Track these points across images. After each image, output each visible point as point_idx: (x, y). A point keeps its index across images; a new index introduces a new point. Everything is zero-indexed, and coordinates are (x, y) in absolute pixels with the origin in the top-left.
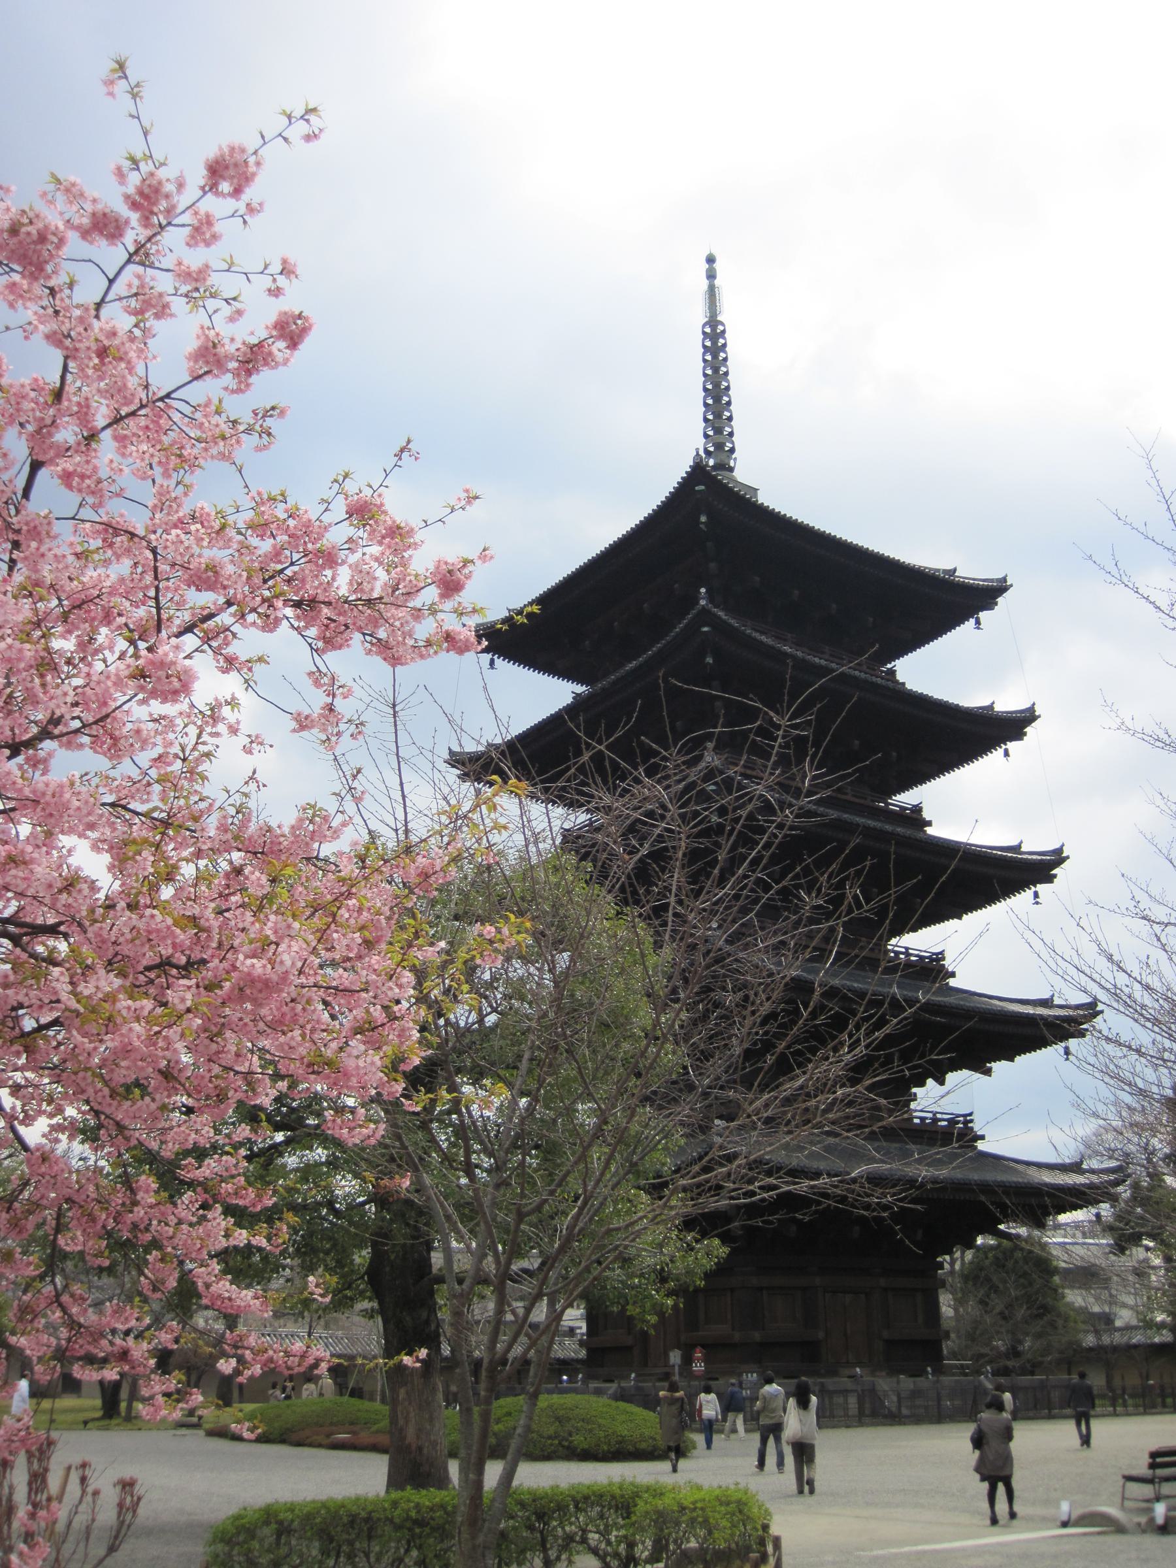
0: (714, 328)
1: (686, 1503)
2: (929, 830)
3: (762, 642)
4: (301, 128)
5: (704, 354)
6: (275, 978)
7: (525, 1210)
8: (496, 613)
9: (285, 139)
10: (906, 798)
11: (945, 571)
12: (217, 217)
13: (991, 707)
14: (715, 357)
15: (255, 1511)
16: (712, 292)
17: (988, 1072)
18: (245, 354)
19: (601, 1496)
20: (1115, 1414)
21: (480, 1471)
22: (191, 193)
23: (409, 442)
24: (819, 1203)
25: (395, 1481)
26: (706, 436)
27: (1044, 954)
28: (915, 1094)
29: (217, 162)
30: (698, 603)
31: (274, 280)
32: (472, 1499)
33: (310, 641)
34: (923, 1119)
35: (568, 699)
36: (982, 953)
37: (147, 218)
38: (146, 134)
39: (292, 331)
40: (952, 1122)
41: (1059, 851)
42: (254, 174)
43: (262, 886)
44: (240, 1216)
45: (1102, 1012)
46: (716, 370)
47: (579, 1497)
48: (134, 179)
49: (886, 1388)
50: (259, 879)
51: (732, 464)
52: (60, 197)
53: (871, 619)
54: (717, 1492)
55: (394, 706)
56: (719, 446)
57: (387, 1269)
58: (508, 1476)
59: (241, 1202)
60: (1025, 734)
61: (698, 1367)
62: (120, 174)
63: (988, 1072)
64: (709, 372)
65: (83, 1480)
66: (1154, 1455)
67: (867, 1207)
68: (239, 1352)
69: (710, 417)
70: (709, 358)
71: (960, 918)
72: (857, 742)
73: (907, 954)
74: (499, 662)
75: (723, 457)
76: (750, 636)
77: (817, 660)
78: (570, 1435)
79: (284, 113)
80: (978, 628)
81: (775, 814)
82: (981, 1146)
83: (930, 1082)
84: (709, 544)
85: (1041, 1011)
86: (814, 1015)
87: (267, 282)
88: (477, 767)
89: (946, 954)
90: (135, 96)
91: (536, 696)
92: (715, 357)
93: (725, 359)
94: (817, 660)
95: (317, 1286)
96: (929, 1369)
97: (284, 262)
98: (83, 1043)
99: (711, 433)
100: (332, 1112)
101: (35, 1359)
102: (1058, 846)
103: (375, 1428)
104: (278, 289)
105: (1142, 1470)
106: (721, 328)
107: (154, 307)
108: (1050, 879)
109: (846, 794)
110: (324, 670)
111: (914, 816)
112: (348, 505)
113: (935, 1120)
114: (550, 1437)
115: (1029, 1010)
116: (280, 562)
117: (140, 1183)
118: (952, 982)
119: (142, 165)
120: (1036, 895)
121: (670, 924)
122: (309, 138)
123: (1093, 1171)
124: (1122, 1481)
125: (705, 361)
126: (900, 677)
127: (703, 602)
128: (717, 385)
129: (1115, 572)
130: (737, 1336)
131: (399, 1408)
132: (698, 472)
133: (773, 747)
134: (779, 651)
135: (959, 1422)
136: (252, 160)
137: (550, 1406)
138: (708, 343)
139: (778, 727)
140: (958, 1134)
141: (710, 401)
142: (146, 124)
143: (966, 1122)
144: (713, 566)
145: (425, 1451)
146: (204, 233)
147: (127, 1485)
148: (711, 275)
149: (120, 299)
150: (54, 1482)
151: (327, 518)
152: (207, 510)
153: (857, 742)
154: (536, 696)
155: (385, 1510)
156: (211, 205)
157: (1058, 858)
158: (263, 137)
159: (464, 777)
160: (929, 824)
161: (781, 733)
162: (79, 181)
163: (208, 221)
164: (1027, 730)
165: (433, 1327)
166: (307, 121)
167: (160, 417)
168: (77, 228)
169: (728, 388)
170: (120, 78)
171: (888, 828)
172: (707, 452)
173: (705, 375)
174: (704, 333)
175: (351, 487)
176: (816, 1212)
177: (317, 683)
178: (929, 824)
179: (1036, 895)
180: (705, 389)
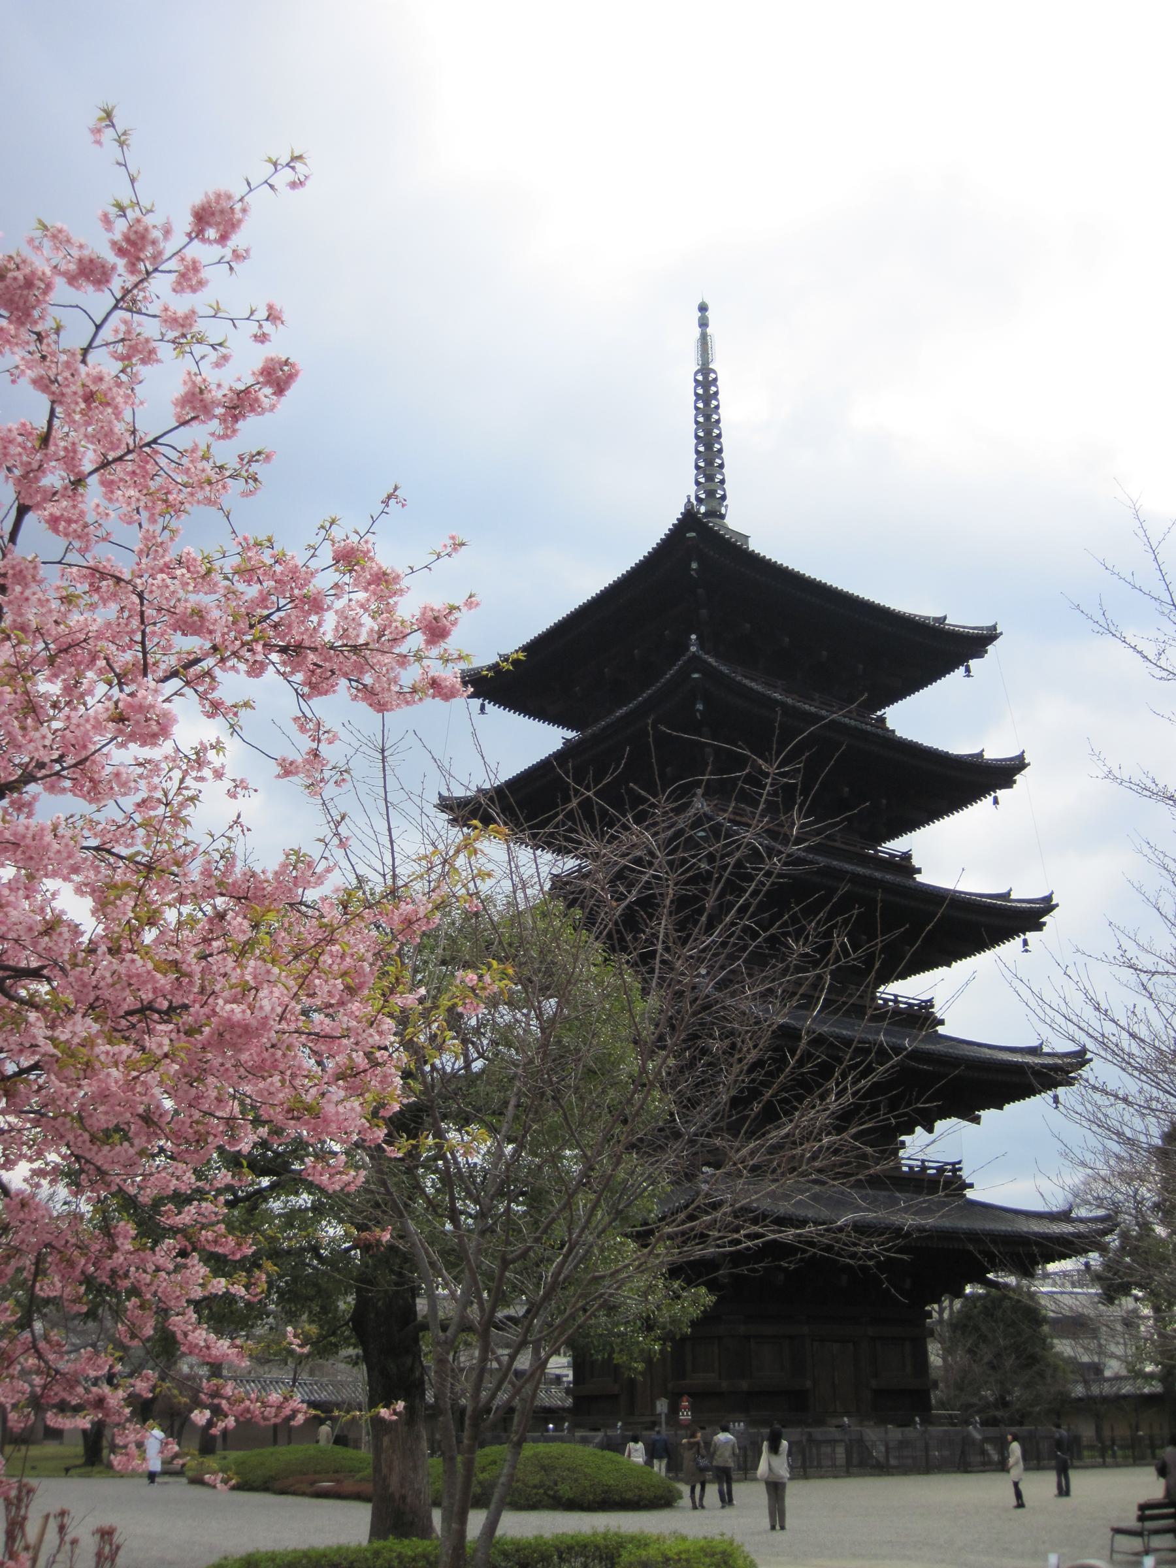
0: (706, 376)
1: (670, 1554)
3: (752, 689)
4: (286, 175)
5: (696, 402)
6: (254, 1023)
7: (510, 1257)
8: (484, 658)
9: (271, 186)
11: (936, 619)
12: (204, 263)
13: (981, 754)
14: (707, 404)
15: (236, 1561)
16: (704, 340)
17: (976, 1120)
18: (232, 400)
19: (585, 1546)
20: (1104, 1465)
21: (463, 1521)
22: (178, 239)
23: (396, 489)
24: (804, 1251)
25: (377, 1531)
26: (698, 483)
27: (1033, 1003)
28: (903, 1143)
29: (203, 209)
30: (688, 649)
31: (261, 326)
32: (455, 1549)
33: (296, 686)
34: (911, 1167)
35: (558, 745)
36: (971, 1000)
37: (134, 265)
38: (133, 181)
39: (278, 377)
40: (940, 1170)
41: (1049, 898)
42: (240, 221)
43: (244, 932)
44: (219, 1264)
45: (1091, 1060)
46: (708, 418)
47: (563, 1547)
48: (121, 226)
49: (874, 1438)
50: (241, 924)
51: (723, 511)
52: (47, 244)
53: (861, 666)
54: (702, 1543)
55: (383, 751)
56: (711, 494)
57: (372, 1316)
58: (492, 1525)
59: (220, 1250)
60: (1015, 782)
61: (685, 1416)
62: (106, 220)
63: (976, 1120)
64: (701, 419)
65: (62, 1528)
66: (1143, 1507)
67: (853, 1256)
68: (216, 1401)
69: (702, 464)
70: (700, 405)
71: (949, 965)
72: (847, 789)
73: (896, 1001)
74: (490, 707)
75: (714, 504)
76: (739, 683)
77: (807, 707)
78: (556, 1484)
79: (270, 160)
80: (968, 676)
81: (763, 862)
82: (970, 1194)
83: (919, 1130)
84: (700, 591)
85: (1029, 1059)
86: (801, 1063)
87: (253, 328)
88: (467, 811)
89: (935, 1002)
90: (122, 144)
91: (525, 742)
92: (707, 404)
93: (717, 407)
94: (807, 707)
95: (296, 1336)
96: (917, 1419)
97: (270, 308)
98: (61, 1088)
99: (702, 480)
100: (312, 1159)
101: (9, 1407)
102: (1047, 894)
103: (358, 1476)
104: (264, 335)
105: (1131, 1522)
106: (713, 376)
107: (140, 352)
108: (1039, 927)
109: (835, 841)
110: (310, 715)
111: (904, 863)
112: (335, 552)
113: (924, 1168)
114: (535, 1487)
115: (1018, 1058)
116: (267, 608)
117: (119, 1229)
118: (941, 1030)
119: (129, 212)
120: (1025, 943)
121: (657, 971)
122: (294, 185)
123: (1081, 1220)
124: (1110, 1534)
125: (697, 408)
126: (890, 725)
127: (693, 649)
128: (708, 433)
129: (1102, 621)
130: (725, 1385)
131: (383, 1456)
132: (689, 519)
133: (761, 795)
134: (769, 698)
135: (948, 1472)
136: (238, 206)
137: (536, 1455)
138: (700, 391)
139: (767, 775)
140: (947, 1182)
141: (702, 449)
142: (133, 171)
143: (954, 1171)
144: (703, 612)
145: (409, 1500)
146: (190, 279)
147: (106, 1534)
148: (703, 324)
149: (107, 344)
150: (32, 1530)
151: (314, 564)
152: (193, 555)
153: (847, 789)
154: (525, 742)
155: (367, 1559)
156: (198, 251)
157: (1046, 906)
158: (249, 184)
159: (454, 822)
160: (919, 871)
161: (769, 781)
162: (65, 227)
163: (195, 267)
164: (1017, 777)
165: (417, 1374)
166: (293, 168)
167: (147, 462)
168: (64, 274)
169: (719, 436)
170: (107, 126)
171: (878, 875)
172: (698, 499)
173: (697, 422)
174: (696, 381)
175: (337, 533)
176: (802, 1260)
177: (303, 729)
178: (919, 871)
179: (1025, 943)
180: (697, 437)
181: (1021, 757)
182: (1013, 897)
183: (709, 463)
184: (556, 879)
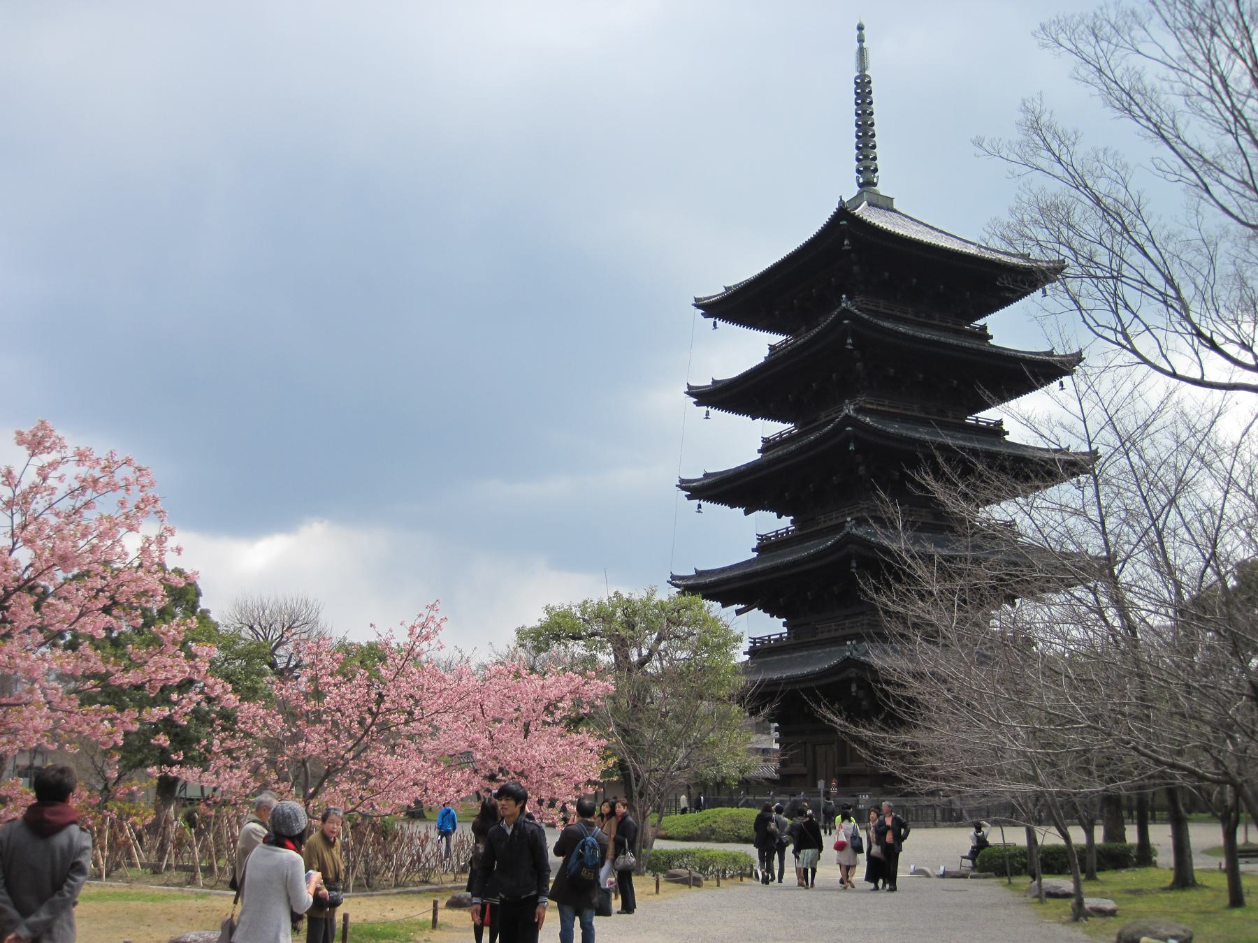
10: (989, 415)
14: (863, 101)
16: (862, 52)
46: (864, 112)
74: (720, 323)
92: (863, 101)
126: (989, 332)
128: (865, 123)
132: (843, 213)
134: (897, 332)
144: (856, 268)
148: (861, 40)
159: (698, 404)
160: (1007, 433)
172: (858, 171)
178: (1007, 433)
181: (1080, 352)
184: (765, 440)
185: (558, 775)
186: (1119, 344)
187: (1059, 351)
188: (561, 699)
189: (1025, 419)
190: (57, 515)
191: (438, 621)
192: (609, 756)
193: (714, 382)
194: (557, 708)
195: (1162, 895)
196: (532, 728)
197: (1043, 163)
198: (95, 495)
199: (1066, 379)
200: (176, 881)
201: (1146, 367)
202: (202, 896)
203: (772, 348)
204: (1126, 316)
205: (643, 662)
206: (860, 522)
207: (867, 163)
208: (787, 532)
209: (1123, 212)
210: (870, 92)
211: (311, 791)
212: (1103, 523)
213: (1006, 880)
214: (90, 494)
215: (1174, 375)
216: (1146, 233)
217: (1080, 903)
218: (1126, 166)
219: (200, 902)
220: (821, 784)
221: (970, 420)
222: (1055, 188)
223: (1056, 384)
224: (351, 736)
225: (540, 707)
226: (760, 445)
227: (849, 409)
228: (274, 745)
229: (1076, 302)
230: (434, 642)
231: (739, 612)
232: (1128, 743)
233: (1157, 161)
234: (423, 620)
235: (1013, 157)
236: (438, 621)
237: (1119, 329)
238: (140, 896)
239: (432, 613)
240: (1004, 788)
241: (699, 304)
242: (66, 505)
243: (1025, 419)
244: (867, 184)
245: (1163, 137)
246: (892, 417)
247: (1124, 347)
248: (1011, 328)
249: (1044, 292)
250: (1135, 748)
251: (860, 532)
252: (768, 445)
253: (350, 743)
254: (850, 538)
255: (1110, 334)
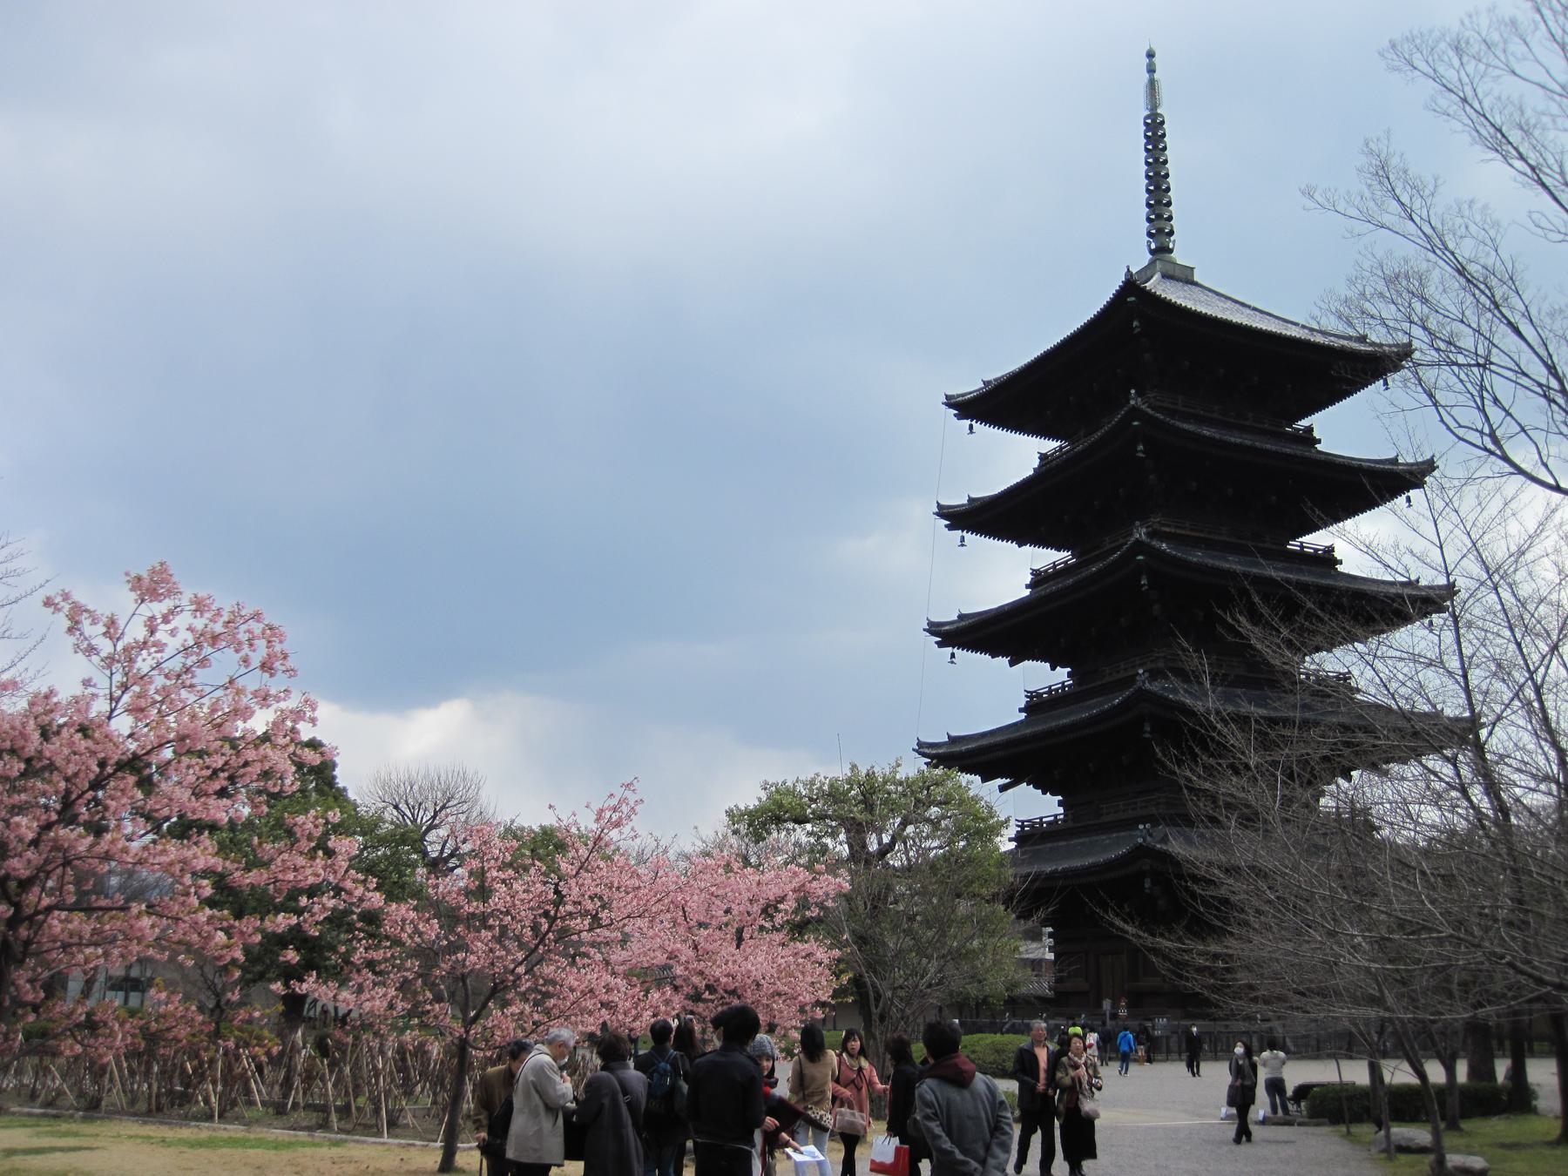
2: (1340, 568)
10: (1316, 540)
14: (1155, 147)
16: (1152, 86)
26: (1149, 220)
74: (977, 426)
92: (1155, 147)
126: (1316, 434)
128: (1157, 174)
132: (1131, 286)
144: (1147, 356)
148: (1151, 70)
159: (950, 527)
160: (1340, 562)
172: (1150, 234)
174: (1146, 124)
178: (1340, 562)
182: (1423, 583)
183: (1159, 202)
184: (1035, 573)
185: (779, 994)
186: (1486, 449)
187: (1407, 458)
188: (782, 899)
189: (1361, 545)
190: (167, 676)
191: (632, 803)
192: (842, 972)
193: (971, 500)
194: (777, 910)
195: (1547, 1152)
196: (746, 935)
197: (1386, 219)
198: (210, 650)
199: (1413, 493)
200: (305, 1123)
201: (1521, 478)
202: (337, 1144)
203: (1043, 457)
204: (1495, 414)
205: (884, 851)
206: (1154, 675)
207: (1161, 224)
208: (1063, 687)
209: (1494, 282)
210: (1164, 135)
211: (472, 1014)
212: (1465, 676)
213: (1343, 1129)
214: (207, 650)
215: (1557, 488)
216: (1523, 309)
217: (1441, 1161)
218: (1496, 224)
219: (336, 1152)
220: (1107, 1005)
221: (1293, 546)
222: (1405, 251)
223: (1401, 500)
224: (521, 946)
225: (756, 909)
226: (1028, 579)
227: (1140, 533)
228: (428, 955)
229: (1431, 396)
230: (626, 830)
231: (1003, 788)
232: (1502, 957)
233: (1535, 216)
234: (614, 802)
235: (1353, 212)
236: (632, 803)
237: (1487, 430)
238: (260, 1143)
239: (628, 794)
240: (1344, 1014)
241: (951, 402)
242: (176, 665)
243: (1361, 545)
244: (1161, 251)
245: (1543, 185)
246: (1195, 543)
247: (1492, 453)
248: (1344, 429)
249: (1386, 383)
250: (1510, 964)
251: (1155, 687)
252: (1039, 579)
253: (520, 956)
254: (1143, 695)
255: (1474, 437)
